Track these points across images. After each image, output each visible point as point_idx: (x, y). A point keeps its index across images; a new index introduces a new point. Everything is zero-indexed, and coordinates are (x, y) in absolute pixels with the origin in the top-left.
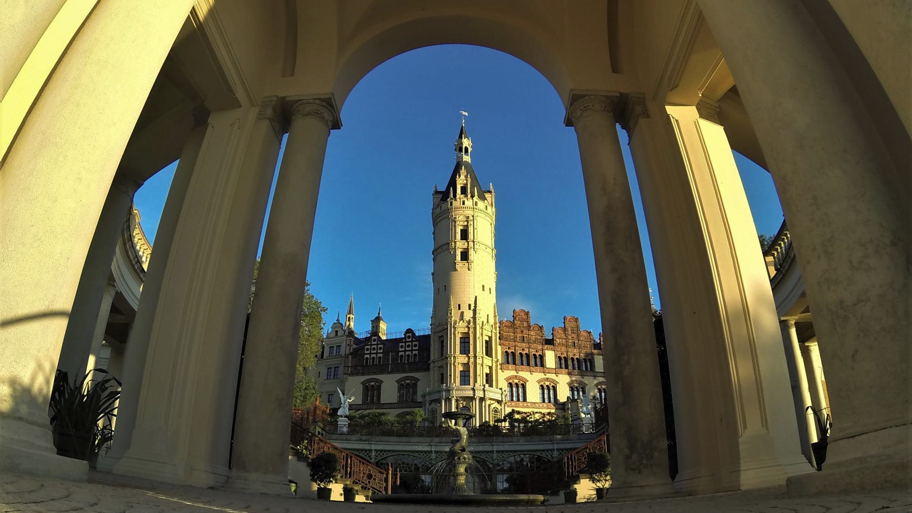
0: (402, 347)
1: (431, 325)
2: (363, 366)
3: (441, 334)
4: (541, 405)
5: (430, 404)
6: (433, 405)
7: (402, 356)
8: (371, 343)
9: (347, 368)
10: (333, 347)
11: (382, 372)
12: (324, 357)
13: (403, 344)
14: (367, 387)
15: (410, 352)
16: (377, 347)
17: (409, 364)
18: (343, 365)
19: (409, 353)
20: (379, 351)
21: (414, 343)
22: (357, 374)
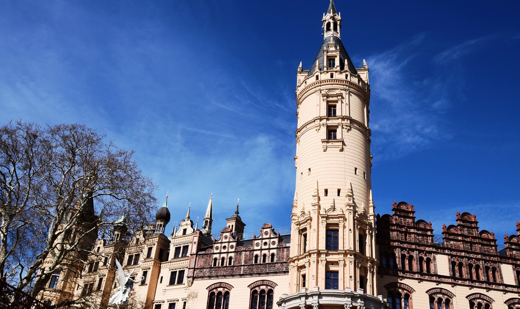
2: (211, 268)
3: (302, 227)
7: (257, 256)
11: (233, 276)
12: (170, 259)
13: (259, 241)
15: (267, 251)
16: (229, 245)
20: (230, 250)
21: (272, 240)
22: (202, 277)
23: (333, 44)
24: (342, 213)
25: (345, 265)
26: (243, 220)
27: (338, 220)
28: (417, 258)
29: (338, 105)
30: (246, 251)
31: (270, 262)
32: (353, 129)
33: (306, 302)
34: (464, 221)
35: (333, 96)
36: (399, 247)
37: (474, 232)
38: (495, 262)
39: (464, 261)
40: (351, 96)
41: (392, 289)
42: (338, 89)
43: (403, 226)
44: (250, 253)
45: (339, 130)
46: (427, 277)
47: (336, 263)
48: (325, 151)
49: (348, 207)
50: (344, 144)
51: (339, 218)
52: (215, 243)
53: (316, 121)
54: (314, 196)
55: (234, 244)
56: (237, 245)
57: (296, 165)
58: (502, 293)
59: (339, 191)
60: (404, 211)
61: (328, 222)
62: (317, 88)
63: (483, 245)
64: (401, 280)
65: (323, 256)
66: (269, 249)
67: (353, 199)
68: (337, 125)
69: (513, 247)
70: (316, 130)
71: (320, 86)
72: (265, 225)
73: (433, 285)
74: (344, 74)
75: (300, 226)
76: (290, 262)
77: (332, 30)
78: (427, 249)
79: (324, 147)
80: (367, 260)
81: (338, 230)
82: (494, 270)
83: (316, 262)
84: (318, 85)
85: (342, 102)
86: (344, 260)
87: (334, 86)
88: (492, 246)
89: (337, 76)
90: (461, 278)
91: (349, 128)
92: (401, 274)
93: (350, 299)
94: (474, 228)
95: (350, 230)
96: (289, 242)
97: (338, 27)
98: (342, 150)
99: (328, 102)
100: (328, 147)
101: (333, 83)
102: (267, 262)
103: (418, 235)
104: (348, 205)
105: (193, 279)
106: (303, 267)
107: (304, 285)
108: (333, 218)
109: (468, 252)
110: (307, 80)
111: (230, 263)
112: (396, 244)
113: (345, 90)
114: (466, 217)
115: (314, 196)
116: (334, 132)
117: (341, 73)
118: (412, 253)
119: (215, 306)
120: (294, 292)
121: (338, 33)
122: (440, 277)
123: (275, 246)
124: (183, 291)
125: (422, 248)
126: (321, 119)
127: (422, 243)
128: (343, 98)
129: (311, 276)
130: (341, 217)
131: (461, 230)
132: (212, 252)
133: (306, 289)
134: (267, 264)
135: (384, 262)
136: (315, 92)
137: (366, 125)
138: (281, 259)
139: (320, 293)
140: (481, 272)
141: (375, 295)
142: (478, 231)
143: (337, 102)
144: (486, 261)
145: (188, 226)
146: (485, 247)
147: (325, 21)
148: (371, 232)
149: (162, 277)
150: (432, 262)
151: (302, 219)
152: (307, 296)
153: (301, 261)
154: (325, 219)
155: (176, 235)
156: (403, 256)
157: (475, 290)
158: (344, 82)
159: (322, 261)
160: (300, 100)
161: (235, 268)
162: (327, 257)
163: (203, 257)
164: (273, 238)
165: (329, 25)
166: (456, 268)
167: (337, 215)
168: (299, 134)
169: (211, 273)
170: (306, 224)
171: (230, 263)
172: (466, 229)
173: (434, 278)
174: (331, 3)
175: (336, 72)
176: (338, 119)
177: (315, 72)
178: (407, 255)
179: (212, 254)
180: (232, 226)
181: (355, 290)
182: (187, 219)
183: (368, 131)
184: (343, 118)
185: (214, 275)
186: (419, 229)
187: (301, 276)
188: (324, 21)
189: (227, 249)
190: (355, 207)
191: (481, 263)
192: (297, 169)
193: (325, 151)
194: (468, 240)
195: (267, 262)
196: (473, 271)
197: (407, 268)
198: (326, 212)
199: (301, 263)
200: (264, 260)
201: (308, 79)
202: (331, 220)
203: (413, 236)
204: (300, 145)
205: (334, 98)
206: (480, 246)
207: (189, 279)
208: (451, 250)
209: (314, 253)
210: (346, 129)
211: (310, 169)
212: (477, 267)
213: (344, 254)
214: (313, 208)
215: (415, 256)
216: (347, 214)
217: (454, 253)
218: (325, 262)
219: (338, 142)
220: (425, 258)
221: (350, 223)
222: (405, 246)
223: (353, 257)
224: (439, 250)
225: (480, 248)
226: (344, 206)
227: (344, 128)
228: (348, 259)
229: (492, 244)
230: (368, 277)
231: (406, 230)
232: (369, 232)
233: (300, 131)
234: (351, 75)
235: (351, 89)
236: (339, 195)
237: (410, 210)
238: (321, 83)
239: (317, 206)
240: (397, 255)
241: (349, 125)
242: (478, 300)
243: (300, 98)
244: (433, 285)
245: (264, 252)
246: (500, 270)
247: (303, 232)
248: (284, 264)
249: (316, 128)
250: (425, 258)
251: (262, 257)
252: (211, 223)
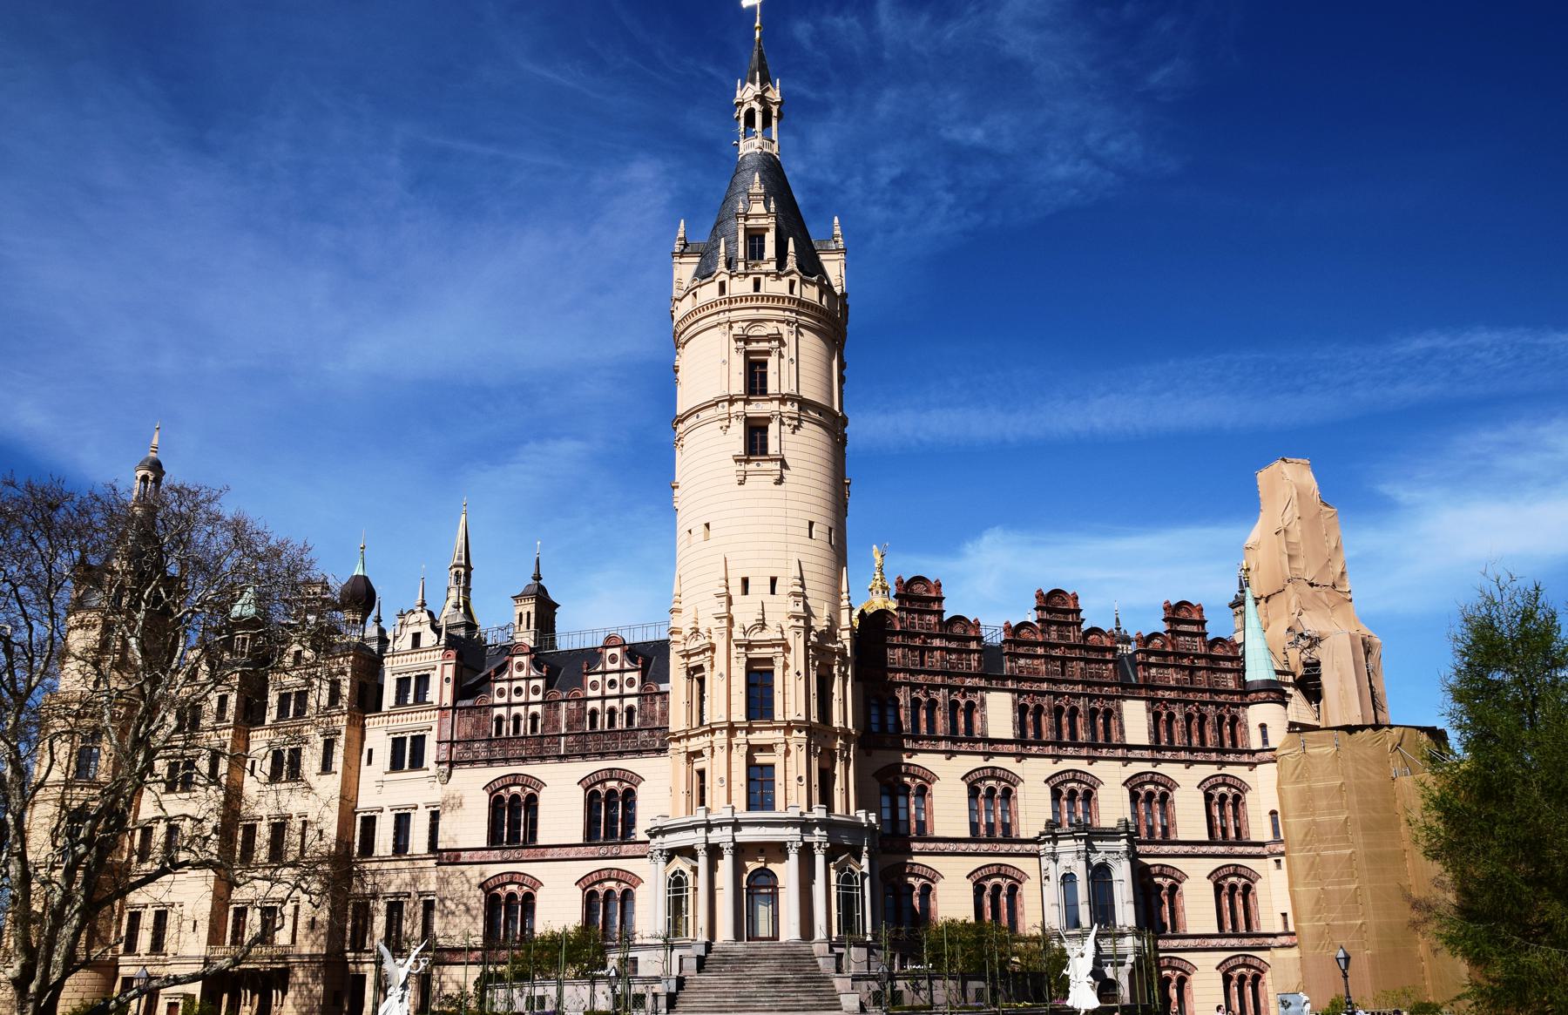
0: (594, 686)
2: (490, 740)
3: (694, 661)
4: (973, 847)
5: (669, 859)
6: (680, 864)
7: (594, 713)
8: (511, 673)
9: (445, 746)
10: (409, 678)
11: (543, 759)
12: (385, 708)
13: (598, 678)
14: (500, 798)
16: (528, 685)
17: (613, 733)
18: (435, 732)
19: (615, 703)
20: (533, 698)
21: (627, 676)
22: (472, 762)
23: (760, 195)
24: (780, 636)
25: (787, 753)
26: (553, 597)
27: (771, 650)
28: (945, 704)
29: (772, 362)
30: (568, 701)
31: (625, 726)
32: (805, 424)
33: (707, 838)
34: (1049, 611)
35: (758, 339)
36: (906, 684)
37: (1072, 634)
38: (1110, 698)
39: (1045, 702)
40: (802, 335)
41: (891, 779)
42: (771, 321)
43: (918, 635)
44: (578, 705)
45: (773, 428)
46: (964, 746)
47: (769, 748)
48: (741, 483)
49: (793, 622)
50: (784, 465)
51: (773, 646)
52: (495, 681)
53: (720, 405)
54: (718, 596)
55: (540, 683)
56: (548, 686)
57: (675, 504)
58: (1120, 763)
59: (773, 581)
60: (921, 599)
61: (750, 656)
62: (723, 317)
63: (1088, 661)
64: (910, 757)
65: (741, 736)
66: (621, 697)
67: (805, 597)
68: (768, 415)
69: (1152, 659)
70: (721, 428)
71: (730, 310)
72: (609, 638)
73: (978, 761)
74: (786, 281)
75: (689, 659)
76: (671, 740)
77: (759, 135)
78: (968, 682)
79: (739, 473)
80: (834, 734)
81: (771, 672)
82: (1108, 714)
83: (726, 748)
84: (720, 308)
85: (781, 356)
86: (786, 742)
87: (761, 311)
88: (1106, 662)
89: (771, 287)
90: (1039, 742)
91: (796, 423)
92: (908, 744)
93: (798, 831)
94: (1073, 624)
95: (798, 674)
96: (667, 681)
97: (774, 122)
98: (780, 481)
99: (747, 354)
101: (759, 304)
102: (618, 727)
103: (949, 651)
104: (794, 617)
105: (451, 767)
106: (699, 754)
107: (702, 803)
108: (760, 647)
109: (1055, 682)
110: (697, 290)
111: (534, 728)
112: (900, 677)
113: (788, 323)
114: (1056, 599)
115: (718, 596)
116: (761, 433)
117: (778, 277)
118: (934, 695)
119: (506, 829)
120: (682, 818)
121: (773, 142)
122: (993, 742)
123: (635, 690)
124: (425, 784)
125: (957, 681)
126: (732, 401)
127: (956, 670)
128: (782, 343)
129: (716, 779)
130: (779, 645)
131: (1042, 631)
132: (489, 703)
133: (708, 811)
134: (619, 731)
135: (874, 719)
136: (715, 326)
137: (836, 408)
138: (649, 720)
139: (737, 819)
140: (1080, 722)
141: (852, 813)
142: (1079, 630)
143: (768, 353)
144: (1091, 697)
145: (423, 626)
146: (1093, 666)
147: (742, 104)
148: (843, 669)
149: (370, 751)
150: (977, 711)
151: (693, 645)
152: (709, 827)
153: (693, 740)
154: (743, 650)
155: (396, 648)
156: (916, 703)
157: (1066, 764)
158: (786, 300)
159: (738, 745)
160: (683, 336)
161: (547, 740)
162: (749, 736)
163: (468, 713)
164: (628, 671)
165: (750, 114)
166: (1029, 718)
167: (770, 640)
168: (681, 428)
169: (491, 751)
170: (702, 656)
171: (534, 728)
172: (1055, 628)
173: (980, 747)
174: (756, 47)
175: (767, 274)
176: (771, 400)
177: (718, 271)
178: (924, 699)
179: (490, 706)
180: (529, 613)
181: (810, 809)
182: (420, 608)
183: (840, 421)
184: (783, 400)
185: (498, 757)
186: (949, 638)
187: (695, 772)
188: (738, 104)
189: (524, 694)
190: (808, 614)
191: (1081, 704)
192: (679, 517)
193: (741, 483)
194: (1057, 652)
195: (618, 727)
196: (1065, 720)
197: (924, 730)
198: (745, 633)
199: (694, 744)
200: (612, 723)
201: (700, 286)
202: (756, 650)
203: (937, 654)
204: (684, 456)
205: (762, 344)
206: (1082, 664)
207: (441, 767)
208: (1019, 679)
209: (721, 729)
210: (789, 425)
211: (707, 525)
212: (1074, 712)
213: (784, 728)
214: (717, 623)
215: (940, 700)
216: (790, 635)
217: (1026, 686)
218: (745, 748)
219: (771, 460)
220: (963, 702)
221: (797, 658)
222: (921, 679)
223: (803, 734)
224: (994, 682)
225: (1082, 669)
226: (785, 617)
227: (784, 424)
228: (793, 740)
229: (1109, 656)
230: (837, 771)
231: (924, 642)
232: (839, 670)
233: (682, 421)
234: (803, 282)
235: (803, 318)
236: (773, 592)
237: (933, 595)
238: (731, 302)
239: (725, 620)
240: (902, 702)
241: (796, 416)
242: (1069, 785)
243: (682, 333)
244: (978, 761)
245: (609, 703)
246: (1120, 714)
247: (695, 672)
248: (657, 733)
249: (719, 424)
250: (963, 702)
251: (607, 716)
252: (468, 576)
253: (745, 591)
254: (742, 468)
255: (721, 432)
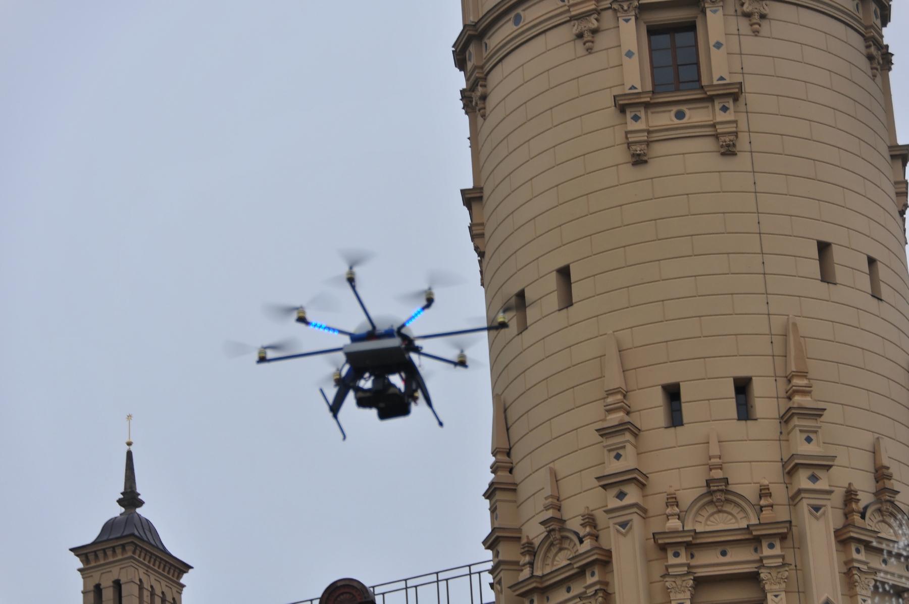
1: (491, 543)
59: (742, 387)
100: (655, 136)
108: (723, 547)
115: (605, 433)
193: (639, 160)
204: (492, 120)
211: (564, 273)
236: (745, 412)
249: (575, 28)
253: (675, 418)
254: (641, 125)
255: (580, 46)
